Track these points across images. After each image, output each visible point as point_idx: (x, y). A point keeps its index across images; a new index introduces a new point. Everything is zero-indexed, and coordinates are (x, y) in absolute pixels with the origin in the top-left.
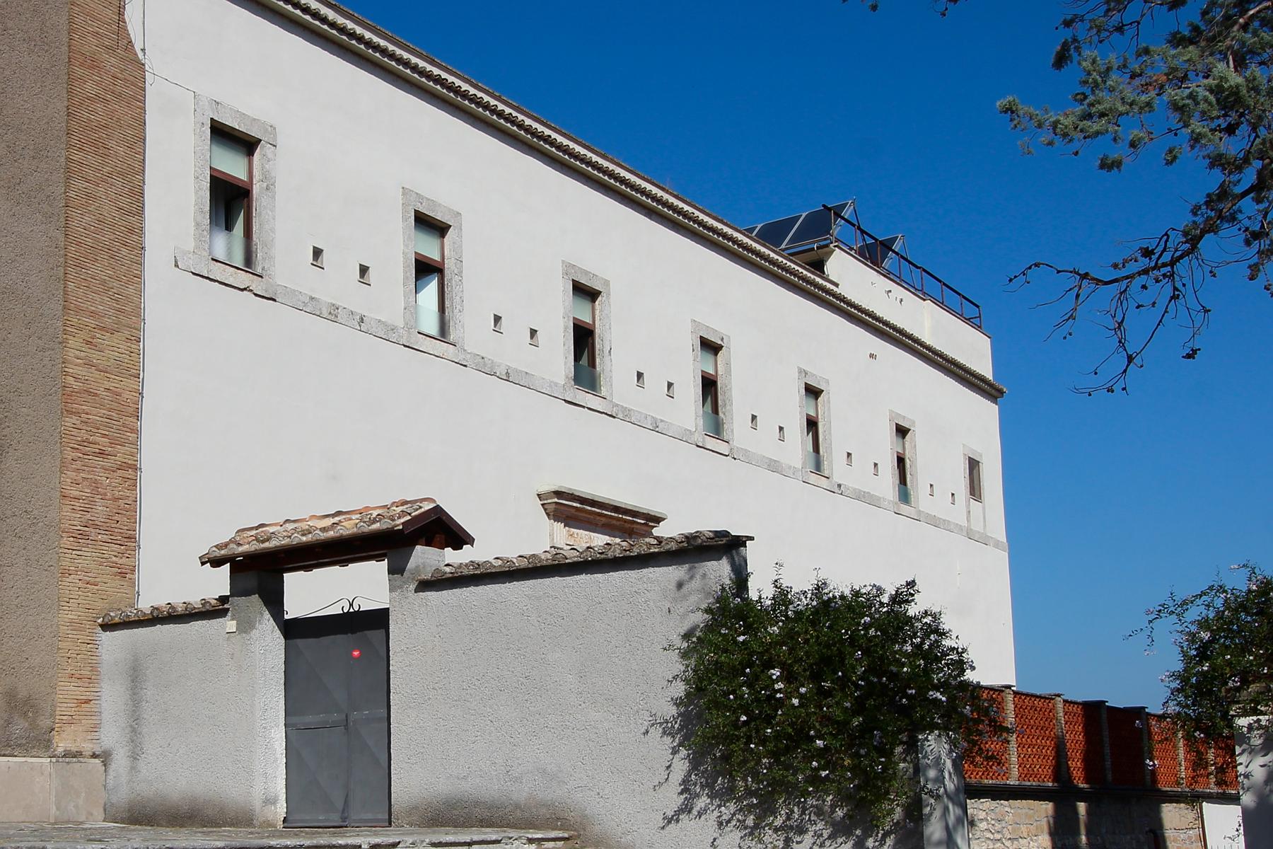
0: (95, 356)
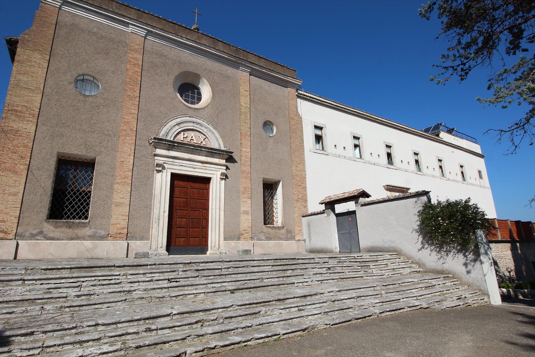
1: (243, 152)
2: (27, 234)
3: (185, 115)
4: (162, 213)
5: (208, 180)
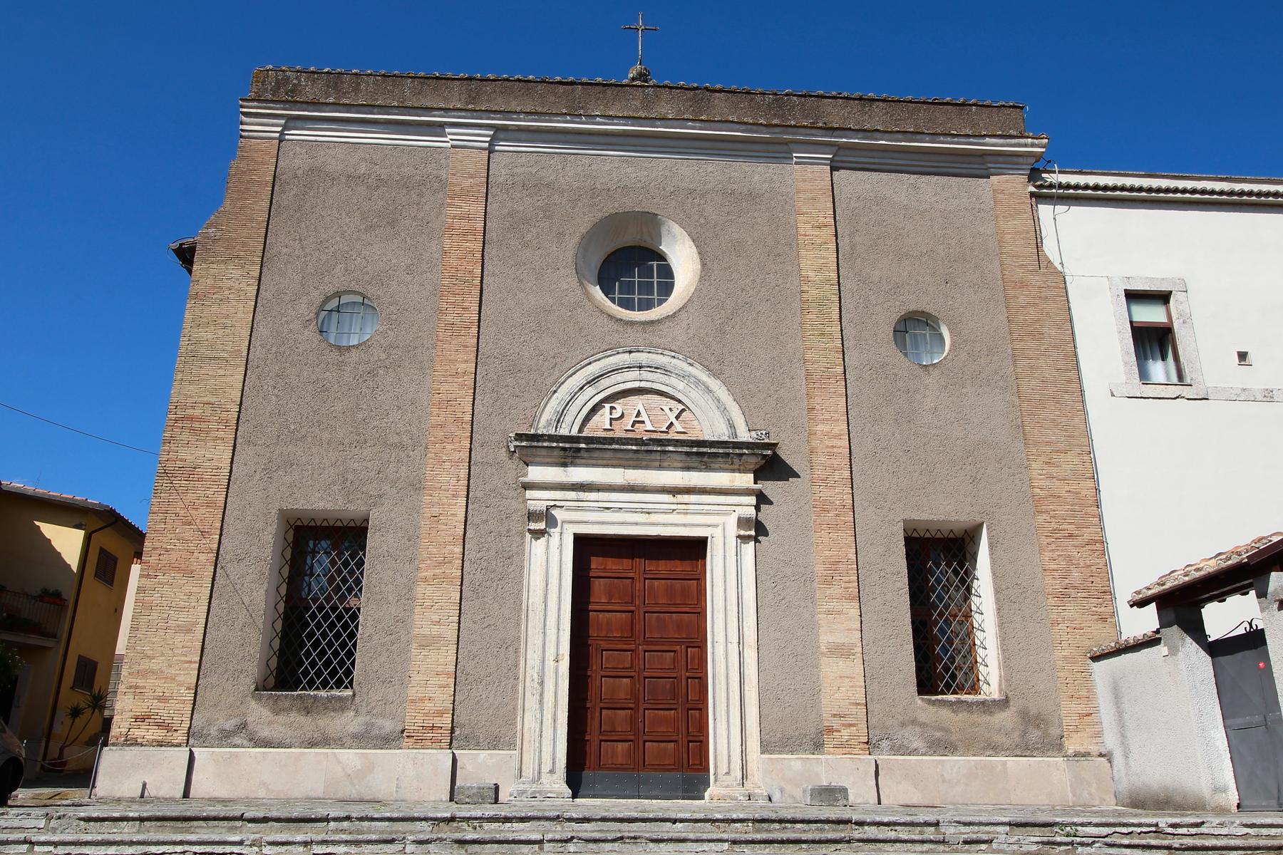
0: (1054, 471)
1: (819, 442)
2: (213, 731)
3: (613, 349)
4: (550, 664)
5: (695, 549)
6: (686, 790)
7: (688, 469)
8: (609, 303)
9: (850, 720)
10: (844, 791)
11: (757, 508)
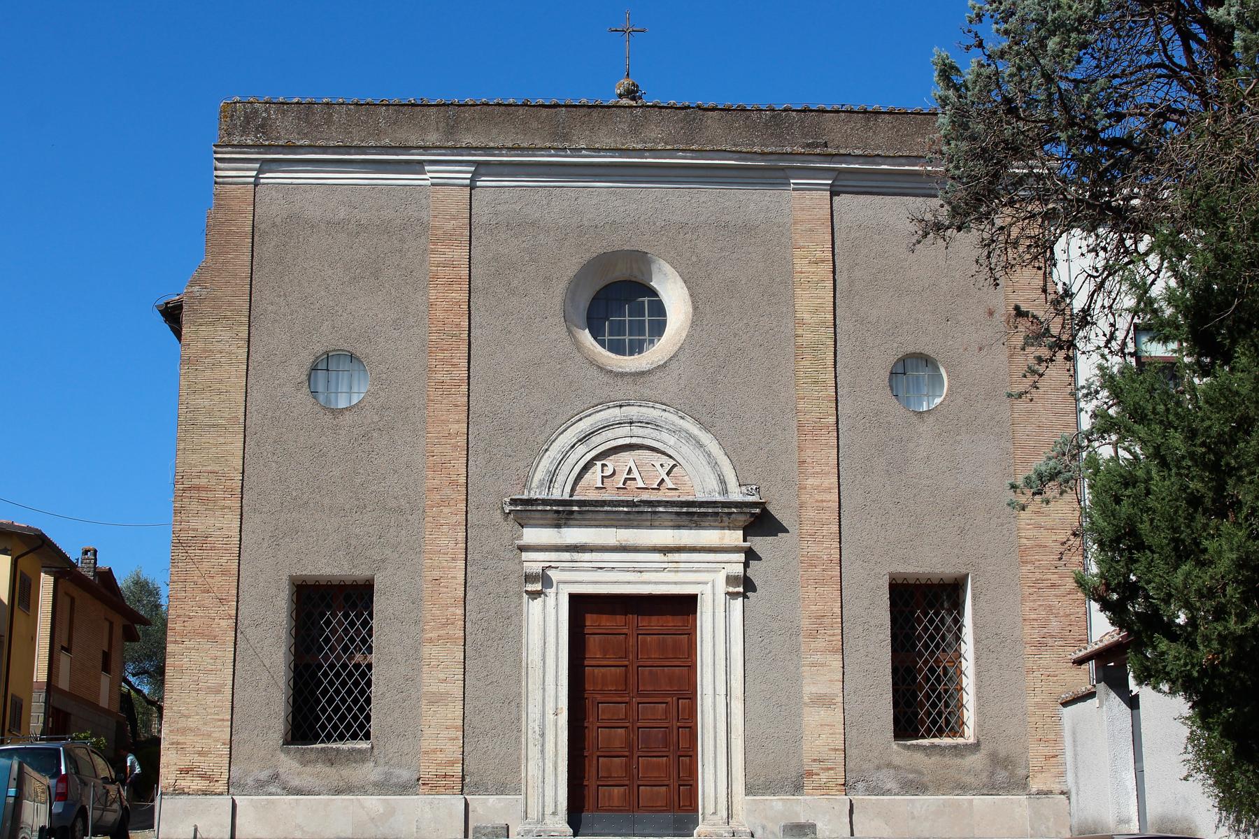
0: (1042, 520)
1: (808, 498)
2: (250, 781)
3: (604, 404)
4: (550, 717)
5: (686, 605)
6: (675, 829)
7: (679, 527)
8: (599, 348)
9: (829, 765)
10: (813, 827)
11: (746, 565)
